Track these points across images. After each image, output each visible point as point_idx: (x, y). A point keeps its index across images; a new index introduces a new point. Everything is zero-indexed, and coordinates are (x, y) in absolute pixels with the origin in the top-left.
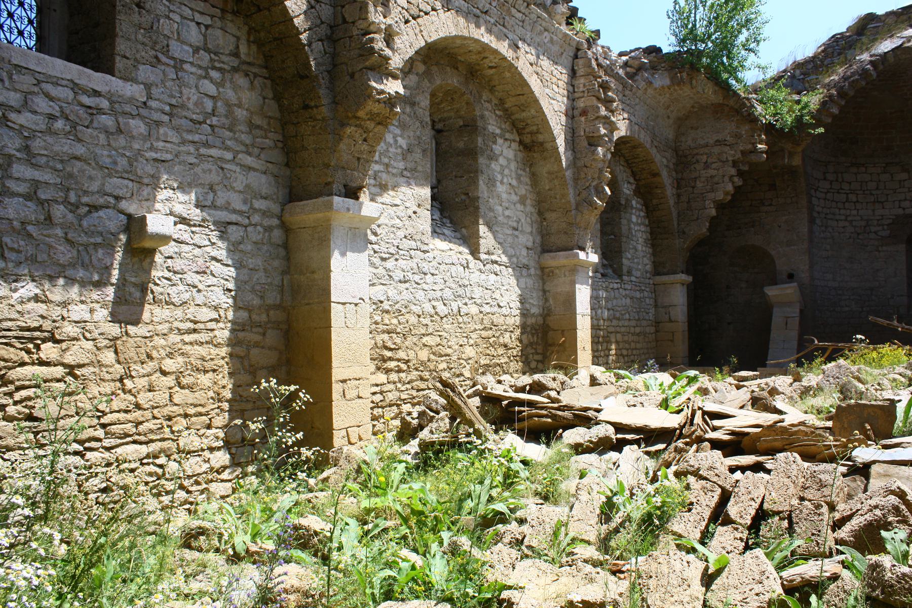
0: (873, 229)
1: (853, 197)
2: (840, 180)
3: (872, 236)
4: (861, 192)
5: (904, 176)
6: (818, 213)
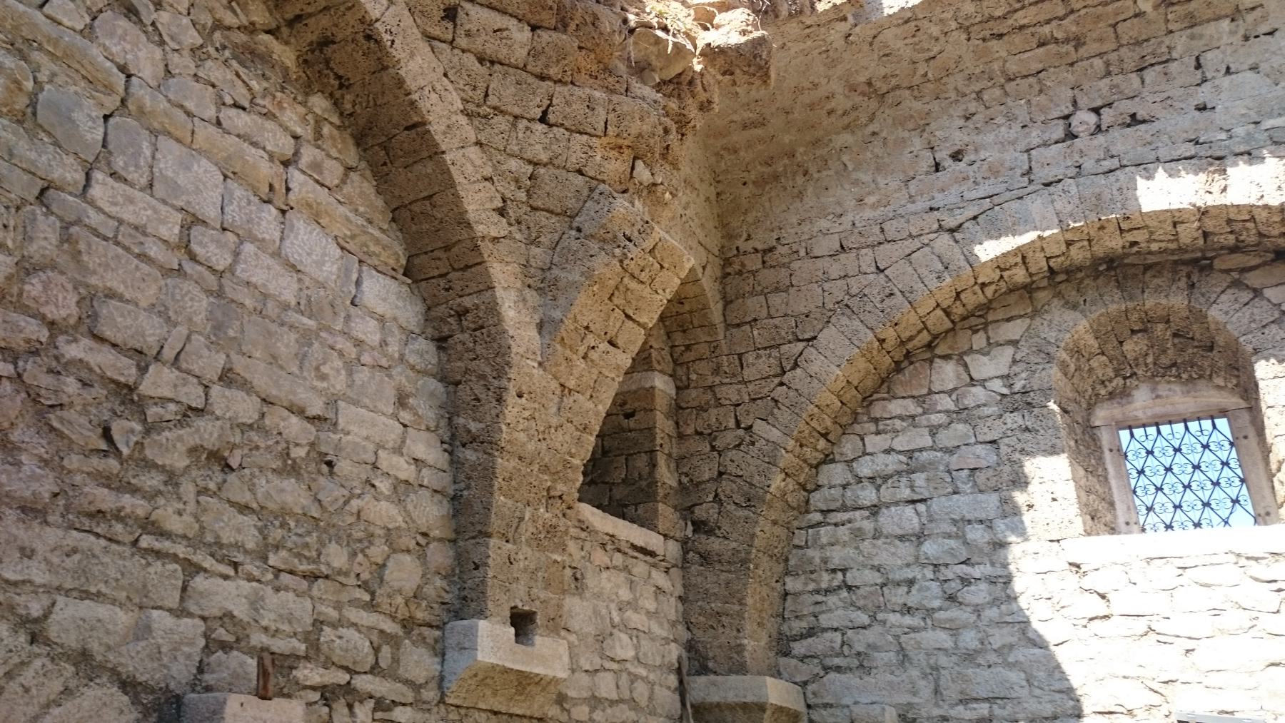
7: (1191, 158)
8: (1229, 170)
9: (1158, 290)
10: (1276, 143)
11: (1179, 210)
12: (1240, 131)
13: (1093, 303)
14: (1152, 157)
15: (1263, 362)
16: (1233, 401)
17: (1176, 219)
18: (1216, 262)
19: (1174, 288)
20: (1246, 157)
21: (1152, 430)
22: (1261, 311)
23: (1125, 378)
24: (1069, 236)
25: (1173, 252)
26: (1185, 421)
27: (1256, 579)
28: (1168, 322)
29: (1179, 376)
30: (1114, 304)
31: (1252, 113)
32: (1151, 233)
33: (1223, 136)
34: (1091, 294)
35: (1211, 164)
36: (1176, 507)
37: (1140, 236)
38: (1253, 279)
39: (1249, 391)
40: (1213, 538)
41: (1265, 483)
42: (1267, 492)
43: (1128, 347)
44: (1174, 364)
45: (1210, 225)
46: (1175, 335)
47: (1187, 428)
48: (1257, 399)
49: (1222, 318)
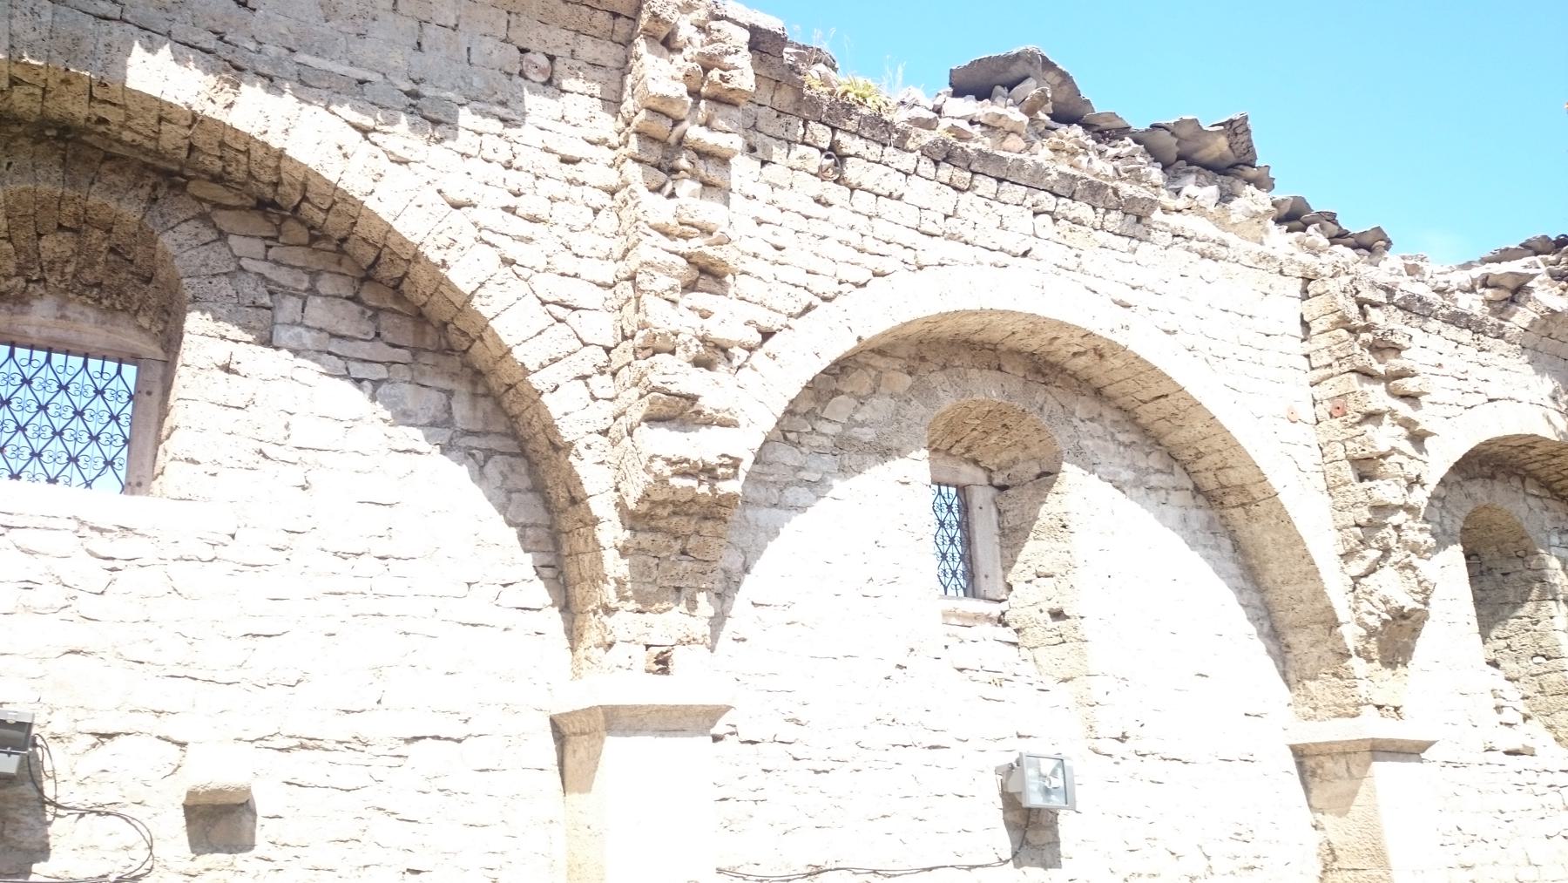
7: (208, 52)
8: (243, 87)
9: (111, 188)
10: (302, 82)
11: (171, 105)
12: (271, 50)
13: (21, 171)
14: (163, 27)
15: (197, 314)
16: (151, 349)
17: (163, 113)
18: (192, 184)
19: (131, 194)
20: (266, 81)
21: (40, 356)
22: (217, 258)
23: (28, 281)
24: (18, 72)
25: (147, 152)
26: (86, 356)
27: (92, 554)
28: (109, 231)
29: (98, 301)
30: (49, 184)
31: (291, 37)
32: (129, 118)
33: (252, 46)
34: (22, 159)
35: (227, 71)
36: (33, 454)
37: (114, 115)
38: (224, 220)
39: (171, 342)
40: (68, 498)
41: (150, 448)
42: (149, 458)
43: (47, 243)
44: (99, 285)
45: (200, 139)
46: (112, 250)
47: (85, 365)
48: (177, 354)
49: (172, 249)
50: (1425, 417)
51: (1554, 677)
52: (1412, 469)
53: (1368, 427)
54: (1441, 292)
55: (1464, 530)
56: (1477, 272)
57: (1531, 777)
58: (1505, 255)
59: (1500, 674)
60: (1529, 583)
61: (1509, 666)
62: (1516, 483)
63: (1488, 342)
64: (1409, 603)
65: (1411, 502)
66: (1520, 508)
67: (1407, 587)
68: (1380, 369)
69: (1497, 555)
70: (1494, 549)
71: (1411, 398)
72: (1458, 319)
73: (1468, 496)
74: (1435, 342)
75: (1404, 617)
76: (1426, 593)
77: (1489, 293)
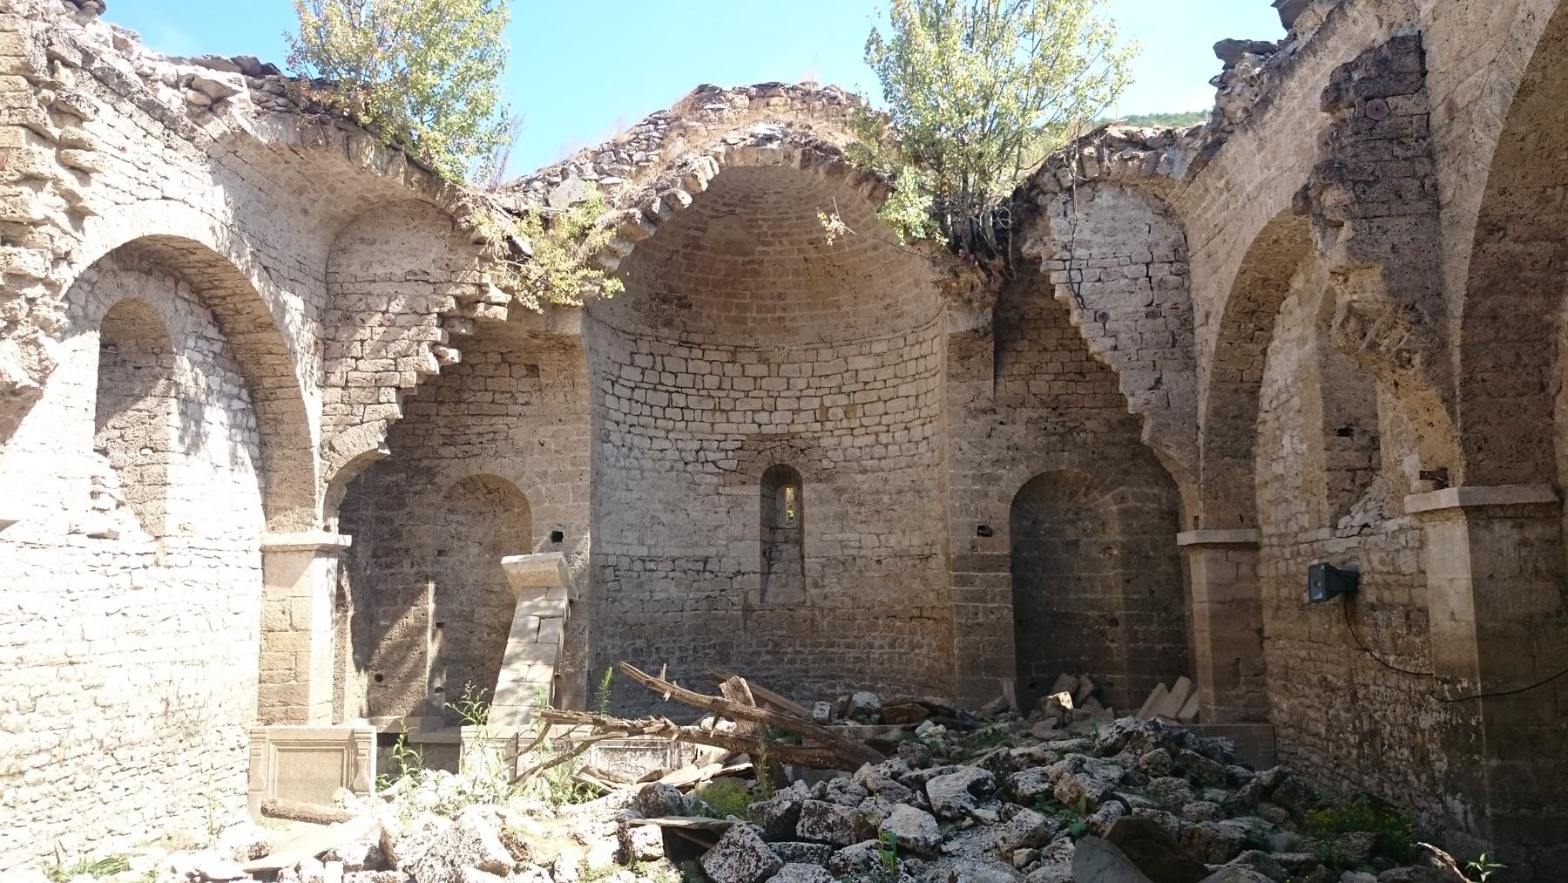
0: (711, 456)
1: (679, 400)
2: (659, 367)
3: (710, 468)
4: (693, 391)
5: (761, 370)
6: (618, 423)
50: (90, 195)
51: (156, 469)
52: (63, 245)
53: (26, 190)
54: (145, 77)
55: (106, 318)
56: (185, 70)
57: (107, 559)
58: (214, 63)
59: (107, 461)
60: (157, 378)
61: (118, 455)
62: (170, 283)
63: (177, 141)
64: (22, 378)
65: (53, 277)
66: (167, 307)
67: (26, 363)
68: (56, 133)
69: (134, 348)
70: (133, 342)
71: (83, 173)
72: (153, 109)
73: (120, 286)
74: (124, 124)
75: (15, 393)
76: (44, 371)
77: (191, 94)
